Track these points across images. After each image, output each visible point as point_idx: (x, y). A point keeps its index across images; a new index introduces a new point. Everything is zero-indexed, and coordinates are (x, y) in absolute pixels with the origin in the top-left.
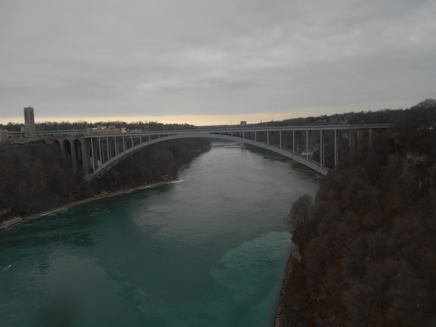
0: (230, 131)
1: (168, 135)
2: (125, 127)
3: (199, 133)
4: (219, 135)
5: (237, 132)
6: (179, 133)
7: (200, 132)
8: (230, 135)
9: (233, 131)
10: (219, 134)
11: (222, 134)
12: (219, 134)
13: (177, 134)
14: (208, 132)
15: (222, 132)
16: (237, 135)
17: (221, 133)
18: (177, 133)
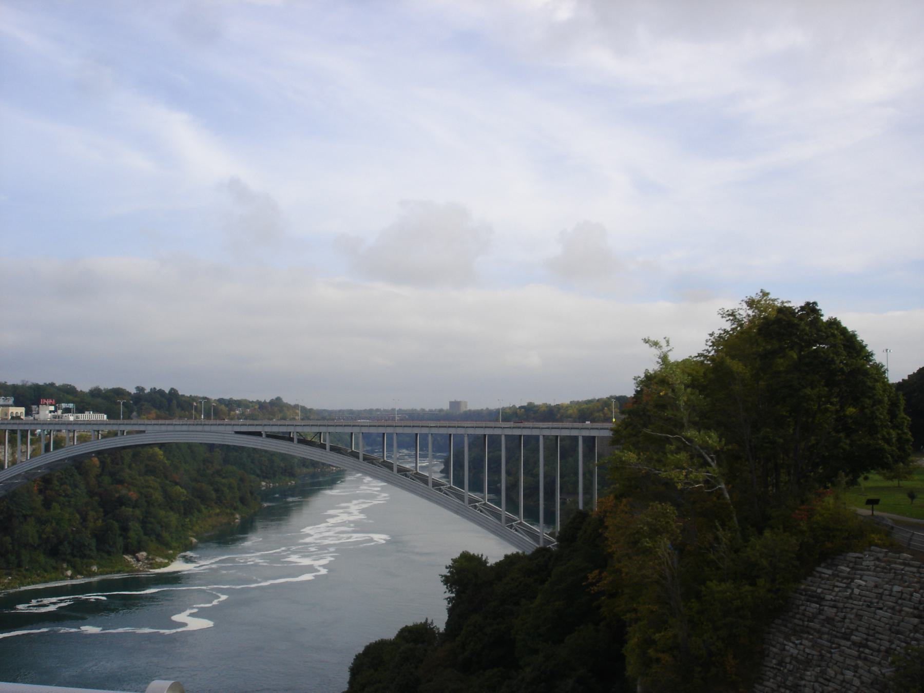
0: (290, 429)
1: (119, 432)
2: (51, 405)
3: (205, 432)
4: (260, 439)
5: (318, 433)
6: (150, 428)
7: (207, 428)
8: (291, 440)
9: (299, 429)
10: (259, 434)
11: (270, 436)
12: (259, 434)
13: (144, 432)
14: (229, 428)
15: (268, 429)
16: (316, 440)
17: (266, 432)
18: (142, 428)
